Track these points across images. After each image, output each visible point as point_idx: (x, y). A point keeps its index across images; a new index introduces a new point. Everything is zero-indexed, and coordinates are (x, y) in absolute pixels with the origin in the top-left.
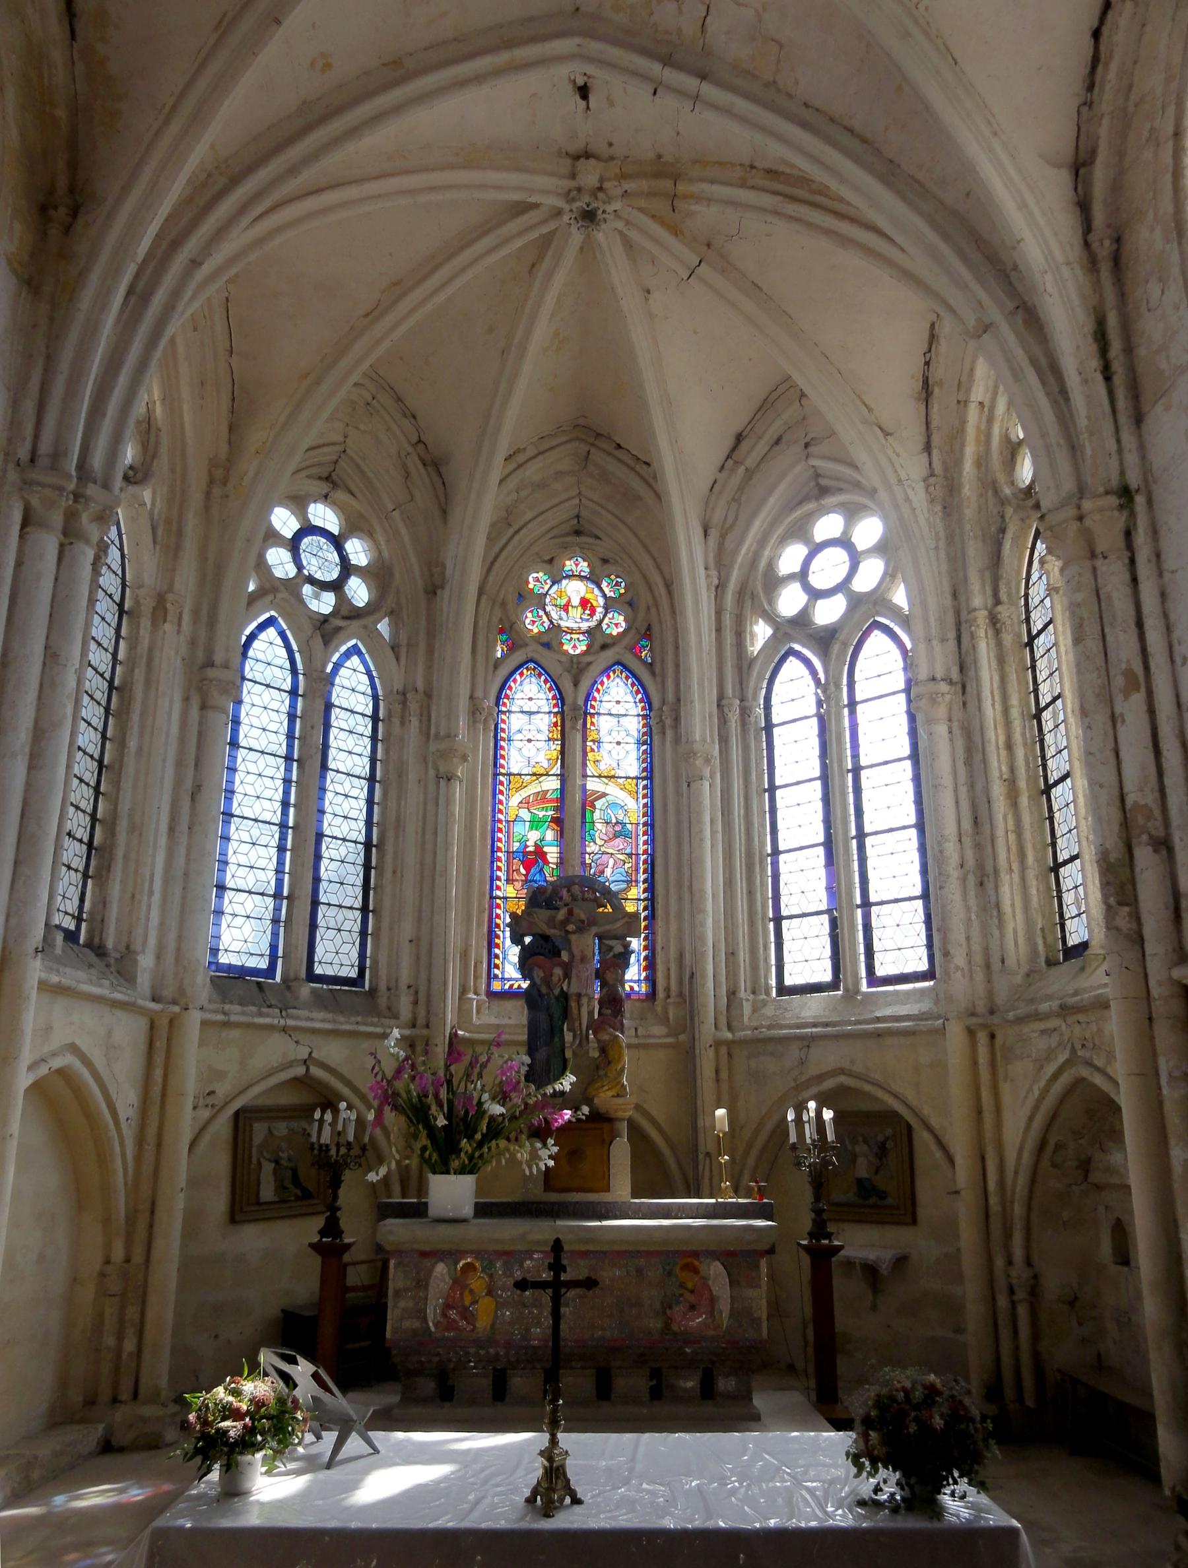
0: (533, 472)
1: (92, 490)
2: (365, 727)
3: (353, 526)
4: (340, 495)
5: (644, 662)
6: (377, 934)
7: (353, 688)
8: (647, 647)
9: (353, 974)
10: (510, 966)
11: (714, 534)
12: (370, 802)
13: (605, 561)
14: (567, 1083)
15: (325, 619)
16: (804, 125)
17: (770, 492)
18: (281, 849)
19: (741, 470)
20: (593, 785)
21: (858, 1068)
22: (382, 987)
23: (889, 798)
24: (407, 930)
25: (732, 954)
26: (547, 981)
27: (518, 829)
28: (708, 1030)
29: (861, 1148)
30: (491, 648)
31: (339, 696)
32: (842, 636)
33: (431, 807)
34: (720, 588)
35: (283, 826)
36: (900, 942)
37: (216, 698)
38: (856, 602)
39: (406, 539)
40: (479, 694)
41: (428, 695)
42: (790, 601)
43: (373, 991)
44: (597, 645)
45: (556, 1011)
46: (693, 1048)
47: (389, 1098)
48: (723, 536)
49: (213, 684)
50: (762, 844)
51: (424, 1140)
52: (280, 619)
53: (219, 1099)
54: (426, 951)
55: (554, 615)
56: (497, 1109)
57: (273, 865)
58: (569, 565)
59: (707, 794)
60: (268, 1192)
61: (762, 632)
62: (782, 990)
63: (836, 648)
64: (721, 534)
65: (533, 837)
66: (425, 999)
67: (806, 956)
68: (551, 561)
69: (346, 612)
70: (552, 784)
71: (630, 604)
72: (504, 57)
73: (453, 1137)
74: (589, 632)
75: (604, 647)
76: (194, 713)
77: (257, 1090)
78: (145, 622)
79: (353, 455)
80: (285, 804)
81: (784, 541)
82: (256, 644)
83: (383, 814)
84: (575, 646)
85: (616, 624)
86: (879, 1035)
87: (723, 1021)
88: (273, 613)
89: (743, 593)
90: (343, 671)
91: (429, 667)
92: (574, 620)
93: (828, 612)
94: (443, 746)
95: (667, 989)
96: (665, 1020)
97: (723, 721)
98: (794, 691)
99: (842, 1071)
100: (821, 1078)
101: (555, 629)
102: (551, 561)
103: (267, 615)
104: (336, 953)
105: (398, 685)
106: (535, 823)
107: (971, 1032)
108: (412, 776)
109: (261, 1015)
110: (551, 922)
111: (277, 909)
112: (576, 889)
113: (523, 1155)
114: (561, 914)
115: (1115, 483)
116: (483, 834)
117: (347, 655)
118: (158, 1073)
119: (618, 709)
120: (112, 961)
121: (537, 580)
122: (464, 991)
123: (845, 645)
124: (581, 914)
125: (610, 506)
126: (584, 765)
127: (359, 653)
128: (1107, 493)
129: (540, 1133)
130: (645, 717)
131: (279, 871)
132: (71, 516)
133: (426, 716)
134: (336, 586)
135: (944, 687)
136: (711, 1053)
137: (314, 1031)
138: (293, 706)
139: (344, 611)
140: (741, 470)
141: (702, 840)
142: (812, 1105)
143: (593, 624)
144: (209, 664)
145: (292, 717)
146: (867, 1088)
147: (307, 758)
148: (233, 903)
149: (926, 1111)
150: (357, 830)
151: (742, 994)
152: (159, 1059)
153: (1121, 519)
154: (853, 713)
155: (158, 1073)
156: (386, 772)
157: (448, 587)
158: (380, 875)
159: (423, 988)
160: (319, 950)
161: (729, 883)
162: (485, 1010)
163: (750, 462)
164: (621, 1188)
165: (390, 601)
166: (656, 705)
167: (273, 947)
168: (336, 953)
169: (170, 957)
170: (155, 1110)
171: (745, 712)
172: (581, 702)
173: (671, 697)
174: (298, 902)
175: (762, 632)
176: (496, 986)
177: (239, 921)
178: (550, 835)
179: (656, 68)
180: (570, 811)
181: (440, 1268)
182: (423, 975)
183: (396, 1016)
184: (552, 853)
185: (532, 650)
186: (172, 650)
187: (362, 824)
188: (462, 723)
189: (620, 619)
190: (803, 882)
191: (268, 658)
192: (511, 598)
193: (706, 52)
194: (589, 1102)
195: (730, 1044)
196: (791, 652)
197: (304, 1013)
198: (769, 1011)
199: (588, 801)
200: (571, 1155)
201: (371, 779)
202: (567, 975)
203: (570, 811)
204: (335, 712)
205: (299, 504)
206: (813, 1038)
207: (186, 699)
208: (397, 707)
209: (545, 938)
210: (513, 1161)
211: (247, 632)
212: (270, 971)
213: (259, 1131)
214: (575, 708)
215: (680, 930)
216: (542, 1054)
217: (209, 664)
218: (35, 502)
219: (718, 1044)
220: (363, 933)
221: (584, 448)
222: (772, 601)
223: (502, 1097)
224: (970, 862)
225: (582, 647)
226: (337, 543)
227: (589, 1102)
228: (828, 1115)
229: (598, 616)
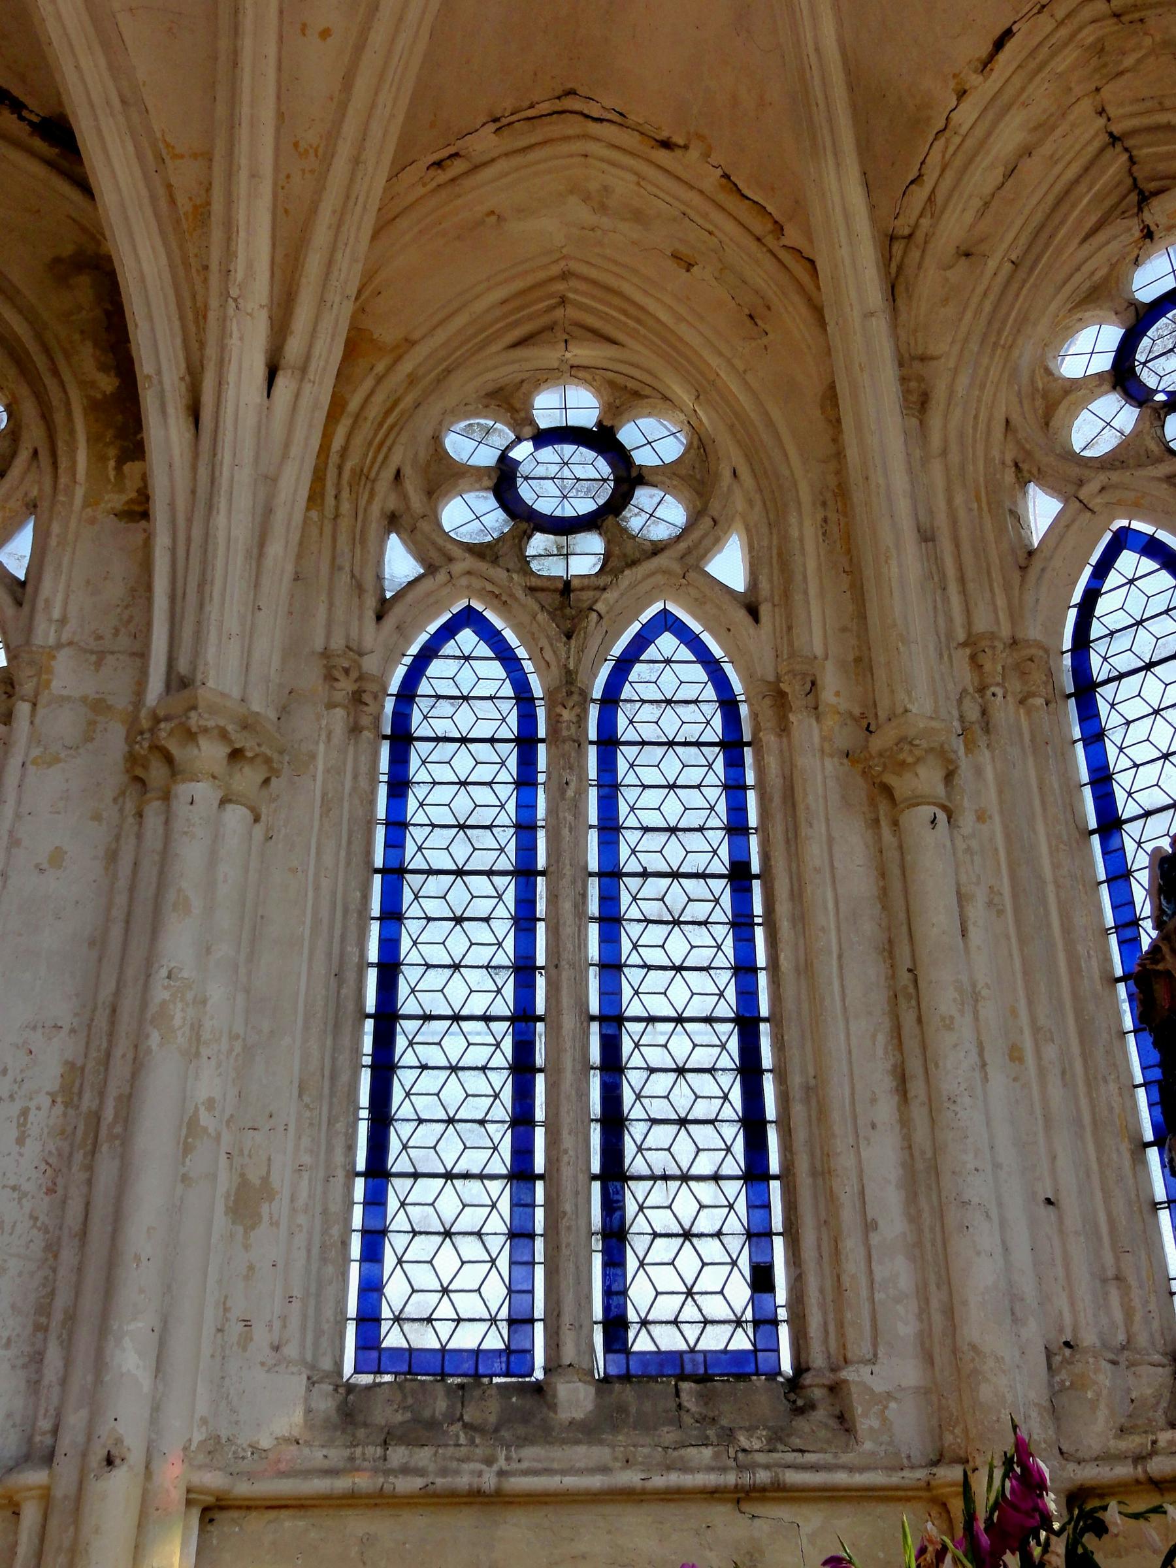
37: (902, 785)
52: (1136, 525)
78: (769, 739)
79: (1135, 122)
82: (1103, 605)
103: (1108, 536)
120: (818, 1393)
169: (941, 1356)
186: (815, 754)
205: (1102, 293)
211: (1077, 597)
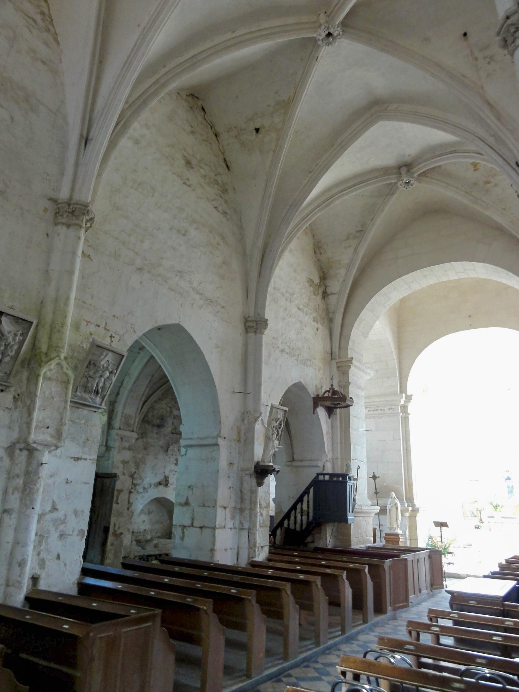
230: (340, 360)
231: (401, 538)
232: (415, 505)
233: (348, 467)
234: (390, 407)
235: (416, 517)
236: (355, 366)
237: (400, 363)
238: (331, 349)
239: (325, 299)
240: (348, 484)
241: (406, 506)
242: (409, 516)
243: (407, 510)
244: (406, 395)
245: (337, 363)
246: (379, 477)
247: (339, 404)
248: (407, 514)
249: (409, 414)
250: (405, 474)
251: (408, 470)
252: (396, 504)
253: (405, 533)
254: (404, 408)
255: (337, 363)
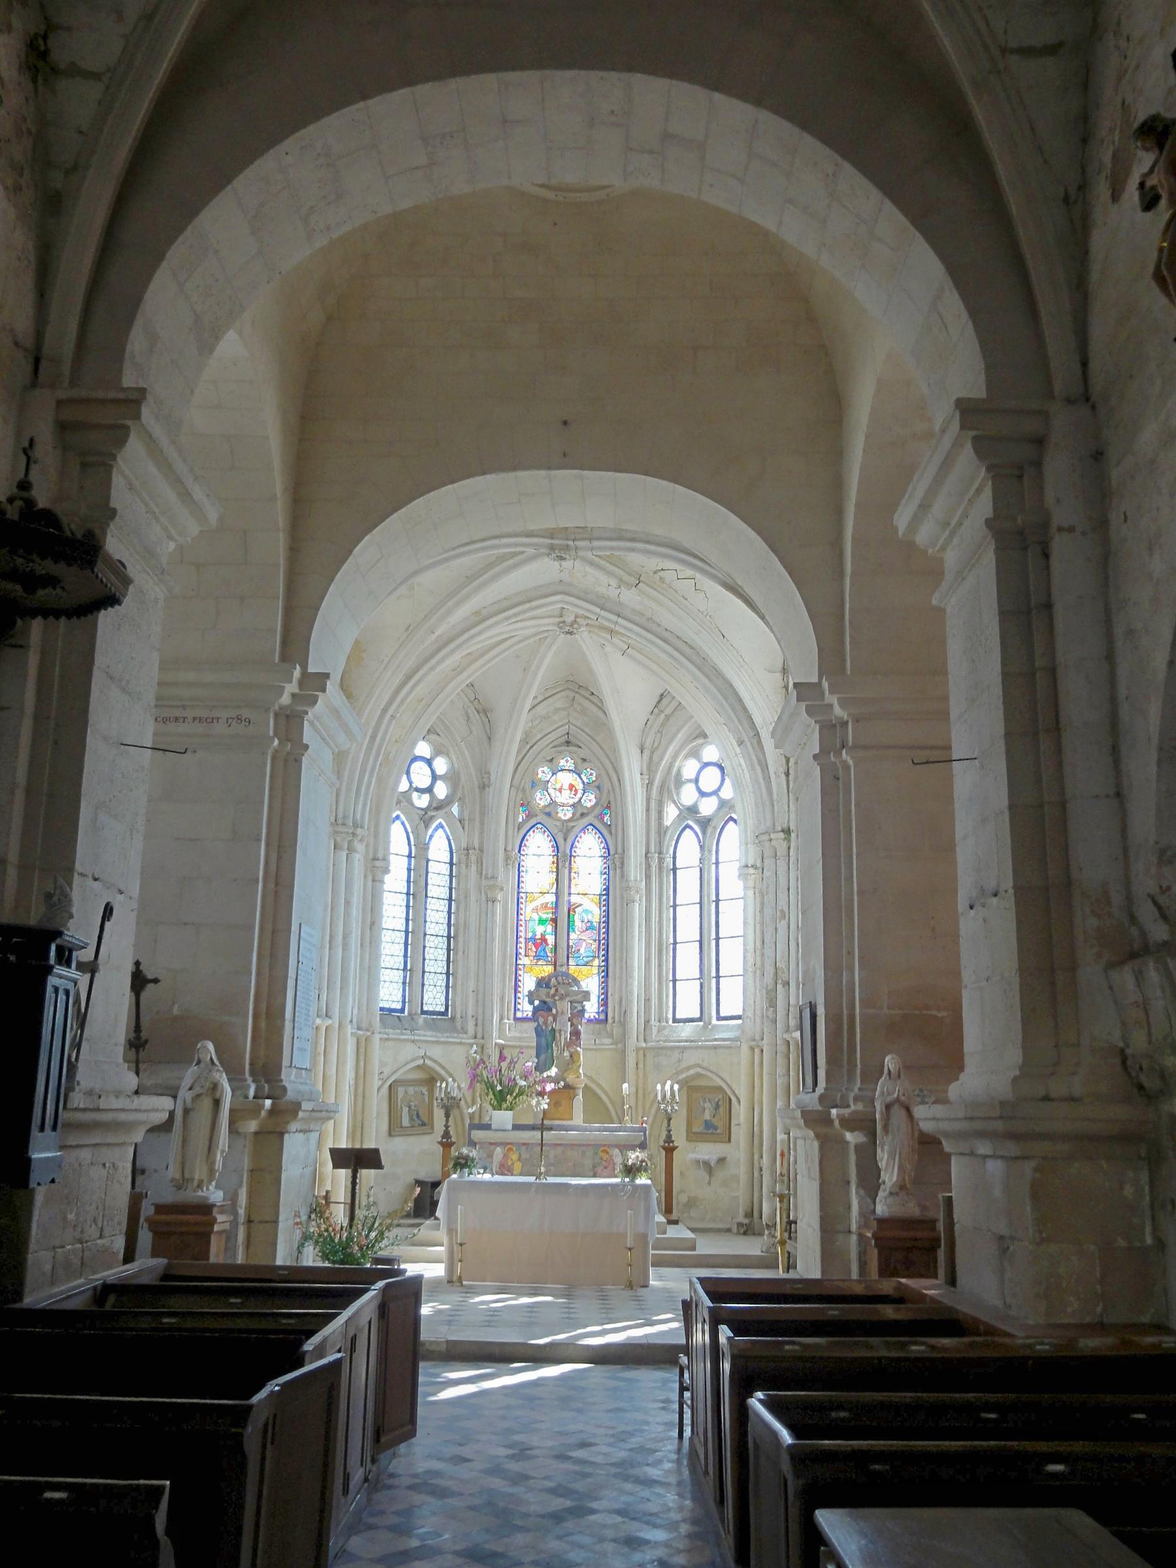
0: (541, 710)
1: (359, 831)
2: (445, 869)
3: (438, 751)
4: (433, 737)
5: (605, 824)
6: (454, 987)
7: (439, 848)
8: (605, 816)
9: (443, 1010)
10: (527, 1009)
11: (647, 753)
12: (449, 913)
13: (584, 760)
14: (553, 1071)
15: (425, 810)
16: (664, 640)
17: (679, 731)
18: (406, 944)
19: (663, 716)
20: (574, 899)
21: (705, 1064)
22: (458, 1016)
23: (734, 918)
24: (472, 984)
25: (647, 1000)
26: (545, 1023)
27: (531, 924)
28: (632, 1042)
29: (707, 1105)
30: (515, 816)
31: (432, 855)
32: (713, 824)
33: (483, 915)
34: (649, 785)
35: (407, 932)
36: (733, 999)
38: (723, 804)
39: (468, 758)
40: (509, 848)
41: (481, 850)
42: (688, 795)
43: (453, 1018)
44: (578, 814)
45: (550, 1039)
46: (624, 1051)
47: (474, 1078)
48: (652, 753)
49: (377, 865)
50: (668, 938)
51: (491, 1096)
52: (402, 817)
53: (384, 1076)
54: (482, 998)
55: (553, 795)
56: (523, 1083)
57: (402, 953)
58: (562, 762)
59: (637, 910)
60: (406, 1122)
61: (671, 813)
62: (675, 1020)
63: (709, 830)
64: (650, 753)
65: (539, 930)
66: (482, 1023)
67: (688, 1005)
68: (551, 760)
69: (438, 806)
70: (551, 898)
71: (598, 787)
72: (528, 606)
73: (502, 1097)
74: (573, 805)
75: (582, 815)
76: (370, 883)
77: (401, 1071)
80: (407, 920)
81: (686, 757)
83: (456, 919)
84: (565, 814)
85: (589, 800)
86: (715, 1047)
87: (641, 1038)
88: (398, 812)
89: (663, 786)
90: (434, 839)
91: (481, 833)
92: (565, 798)
93: (708, 807)
94: (491, 882)
95: (614, 1018)
96: (611, 1036)
97: (648, 867)
98: (688, 849)
99: (698, 1066)
100: (688, 1068)
101: (553, 803)
102: (551, 760)
104: (434, 999)
105: (464, 845)
106: (542, 922)
107: (752, 1049)
108: (473, 899)
109: (402, 1034)
110: (548, 995)
111: (405, 977)
112: (560, 978)
113: (534, 1102)
114: (552, 991)
115: (785, 826)
116: (512, 928)
117: (436, 830)
118: (362, 1063)
119: (589, 846)
121: (543, 773)
122: (501, 1019)
123: (715, 828)
124: (562, 991)
125: (587, 731)
126: (570, 887)
127: (442, 827)
128: (783, 831)
129: (541, 1094)
130: (605, 858)
131: (405, 956)
132: (350, 842)
133: (480, 862)
134: (429, 790)
135: (752, 871)
136: (634, 1054)
137: (427, 1042)
138: (409, 864)
139: (434, 805)
140: (663, 716)
141: (633, 937)
142: (669, 1083)
143: (576, 800)
144: (375, 859)
145: (409, 870)
146: (709, 1074)
147: (416, 893)
148: (385, 975)
149: (734, 1087)
150: (442, 930)
151: (652, 1022)
152: (362, 1058)
153: (785, 844)
154: (717, 868)
155: (362, 1063)
156: (458, 895)
157: (492, 788)
158: (456, 953)
159: (480, 1018)
160: (426, 997)
161: (648, 961)
162: (513, 1028)
163: (668, 711)
164: (578, 1119)
165: (459, 794)
166: (612, 852)
167: (404, 996)
168: (434, 999)
170: (361, 1081)
171: (661, 860)
172: (568, 852)
173: (620, 851)
174: (413, 973)
175: (671, 813)
176: (519, 1015)
177: (387, 984)
178: (550, 928)
179: (598, 610)
180: (561, 915)
181: (498, 1149)
182: (480, 1010)
183: (466, 1033)
184: (551, 939)
185: (539, 819)
187: (445, 926)
188: (501, 869)
189: (592, 797)
190: (687, 961)
191: (398, 839)
192: (528, 786)
193: (620, 604)
194: (564, 1080)
195: (644, 1049)
196: (688, 826)
197: (422, 1032)
198: (666, 1032)
199: (571, 910)
200: (555, 1104)
201: (450, 900)
202: (555, 1020)
203: (561, 915)
204: (430, 863)
206: (685, 1048)
207: (365, 877)
208: (463, 858)
209: (545, 1003)
210: (530, 1105)
212: (402, 1010)
213: (401, 1091)
214: (565, 855)
215: (621, 985)
216: (543, 1057)
217: (375, 859)
218: (339, 839)
219: (638, 1050)
220: (447, 987)
221: (571, 694)
222: (678, 794)
223: (525, 1078)
224: (759, 963)
225: (569, 815)
226: (429, 762)
227: (564, 1080)
228: (676, 1087)
229: (579, 795)
230: (76, 393)
231: (220, 1218)
232: (284, 1089)
233: (58, 902)
234: (233, 713)
235: (281, 1135)
236: (150, 440)
237: (294, 550)
238: (39, 335)
239: (34, 80)
240: (52, 981)
241: (252, 1093)
242: (256, 1133)
243: (256, 1111)
244: (305, 674)
245: (59, 403)
246: (156, 981)
247: (51, 581)
248: (252, 1126)
249: (306, 747)
250: (258, 974)
251: (272, 955)
252: (215, 1086)
253: (234, 1199)
254: (291, 722)
255: (59, 403)
